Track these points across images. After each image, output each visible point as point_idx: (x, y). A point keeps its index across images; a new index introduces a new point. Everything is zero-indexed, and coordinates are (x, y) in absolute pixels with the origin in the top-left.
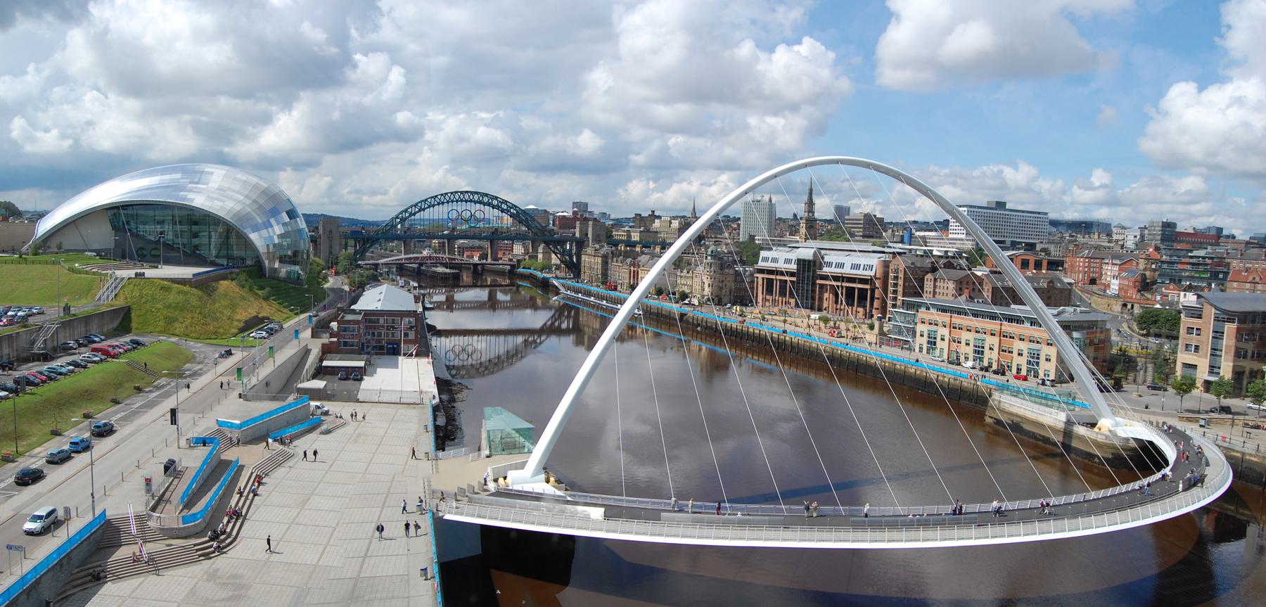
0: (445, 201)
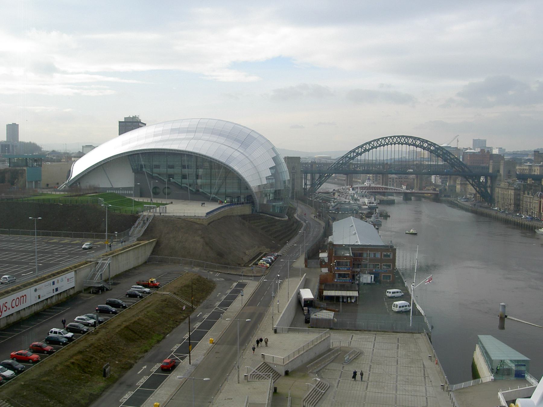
0: (385, 143)
